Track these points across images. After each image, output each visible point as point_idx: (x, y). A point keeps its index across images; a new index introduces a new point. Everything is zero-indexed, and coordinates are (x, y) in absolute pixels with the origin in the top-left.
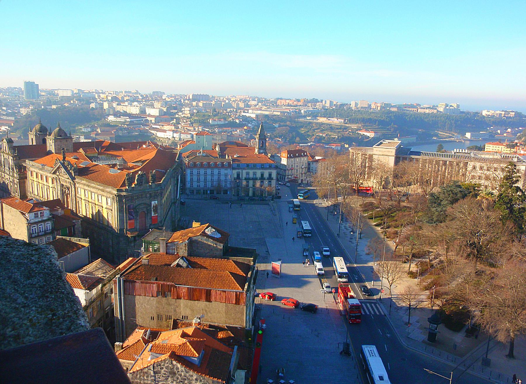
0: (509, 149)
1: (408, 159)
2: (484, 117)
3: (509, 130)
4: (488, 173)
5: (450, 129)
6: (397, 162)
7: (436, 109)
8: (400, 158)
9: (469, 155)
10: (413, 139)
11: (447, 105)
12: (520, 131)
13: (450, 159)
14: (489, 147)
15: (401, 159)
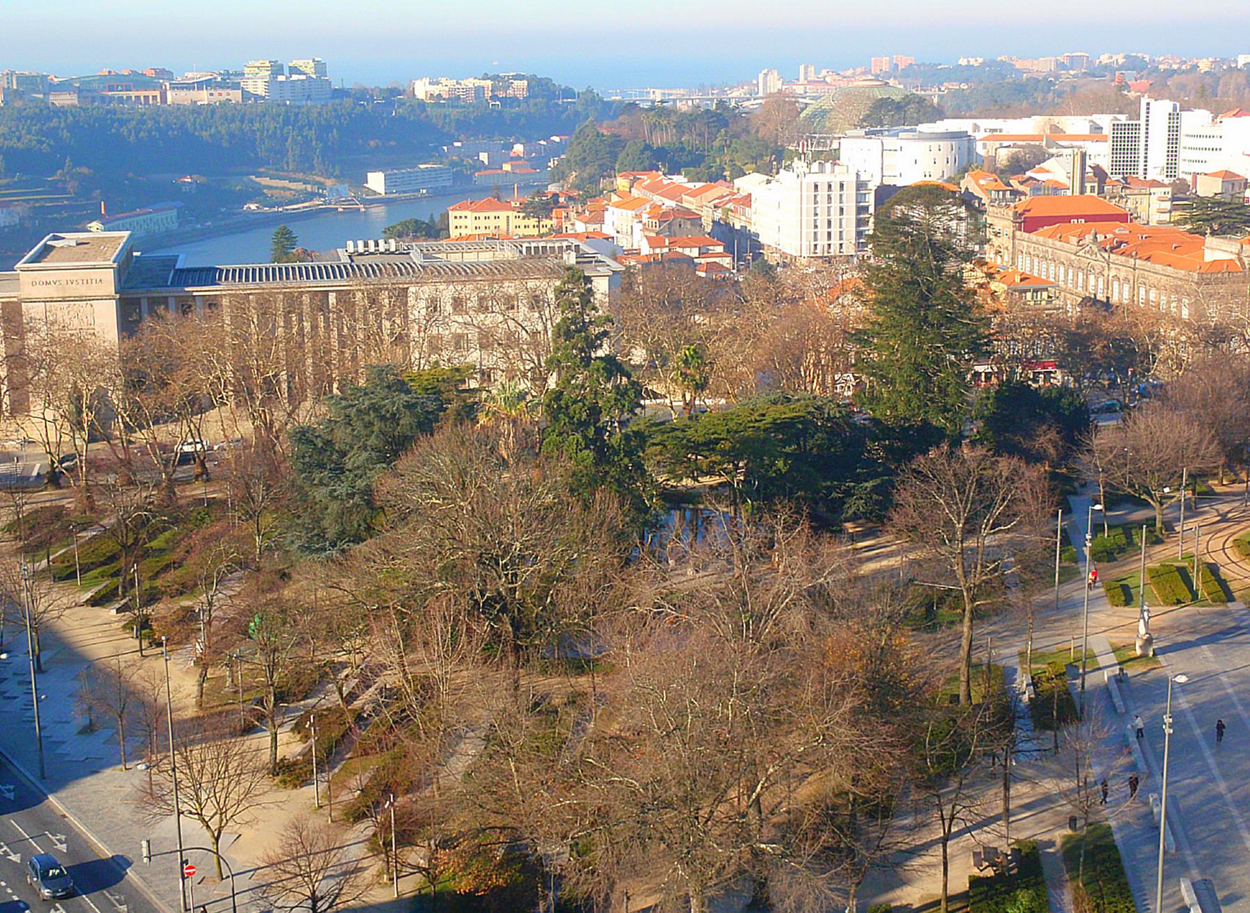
0: (533, 221)
1: (171, 302)
2: (422, 105)
3: (519, 148)
4: (488, 320)
5: (305, 165)
6: (128, 322)
7: (236, 86)
8: (137, 302)
9: (403, 259)
10: (165, 218)
11: (277, 69)
12: (555, 151)
13: (312, 282)
14: (463, 222)
15: (144, 304)
